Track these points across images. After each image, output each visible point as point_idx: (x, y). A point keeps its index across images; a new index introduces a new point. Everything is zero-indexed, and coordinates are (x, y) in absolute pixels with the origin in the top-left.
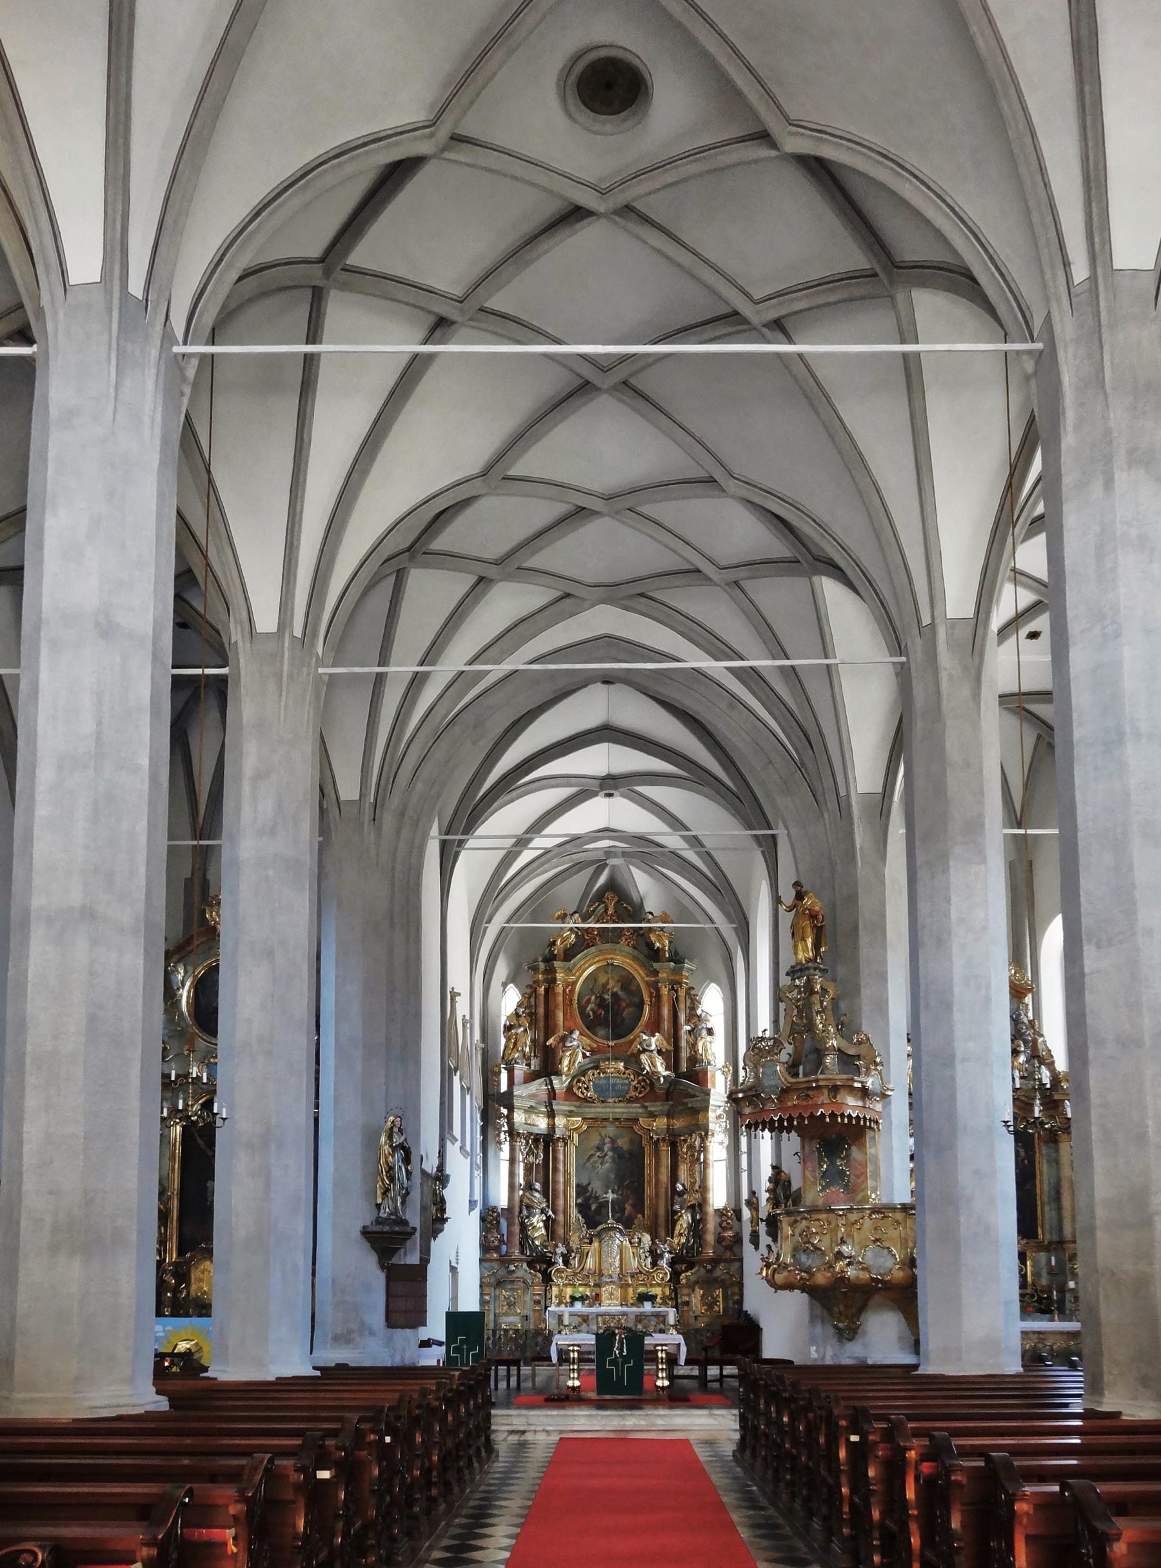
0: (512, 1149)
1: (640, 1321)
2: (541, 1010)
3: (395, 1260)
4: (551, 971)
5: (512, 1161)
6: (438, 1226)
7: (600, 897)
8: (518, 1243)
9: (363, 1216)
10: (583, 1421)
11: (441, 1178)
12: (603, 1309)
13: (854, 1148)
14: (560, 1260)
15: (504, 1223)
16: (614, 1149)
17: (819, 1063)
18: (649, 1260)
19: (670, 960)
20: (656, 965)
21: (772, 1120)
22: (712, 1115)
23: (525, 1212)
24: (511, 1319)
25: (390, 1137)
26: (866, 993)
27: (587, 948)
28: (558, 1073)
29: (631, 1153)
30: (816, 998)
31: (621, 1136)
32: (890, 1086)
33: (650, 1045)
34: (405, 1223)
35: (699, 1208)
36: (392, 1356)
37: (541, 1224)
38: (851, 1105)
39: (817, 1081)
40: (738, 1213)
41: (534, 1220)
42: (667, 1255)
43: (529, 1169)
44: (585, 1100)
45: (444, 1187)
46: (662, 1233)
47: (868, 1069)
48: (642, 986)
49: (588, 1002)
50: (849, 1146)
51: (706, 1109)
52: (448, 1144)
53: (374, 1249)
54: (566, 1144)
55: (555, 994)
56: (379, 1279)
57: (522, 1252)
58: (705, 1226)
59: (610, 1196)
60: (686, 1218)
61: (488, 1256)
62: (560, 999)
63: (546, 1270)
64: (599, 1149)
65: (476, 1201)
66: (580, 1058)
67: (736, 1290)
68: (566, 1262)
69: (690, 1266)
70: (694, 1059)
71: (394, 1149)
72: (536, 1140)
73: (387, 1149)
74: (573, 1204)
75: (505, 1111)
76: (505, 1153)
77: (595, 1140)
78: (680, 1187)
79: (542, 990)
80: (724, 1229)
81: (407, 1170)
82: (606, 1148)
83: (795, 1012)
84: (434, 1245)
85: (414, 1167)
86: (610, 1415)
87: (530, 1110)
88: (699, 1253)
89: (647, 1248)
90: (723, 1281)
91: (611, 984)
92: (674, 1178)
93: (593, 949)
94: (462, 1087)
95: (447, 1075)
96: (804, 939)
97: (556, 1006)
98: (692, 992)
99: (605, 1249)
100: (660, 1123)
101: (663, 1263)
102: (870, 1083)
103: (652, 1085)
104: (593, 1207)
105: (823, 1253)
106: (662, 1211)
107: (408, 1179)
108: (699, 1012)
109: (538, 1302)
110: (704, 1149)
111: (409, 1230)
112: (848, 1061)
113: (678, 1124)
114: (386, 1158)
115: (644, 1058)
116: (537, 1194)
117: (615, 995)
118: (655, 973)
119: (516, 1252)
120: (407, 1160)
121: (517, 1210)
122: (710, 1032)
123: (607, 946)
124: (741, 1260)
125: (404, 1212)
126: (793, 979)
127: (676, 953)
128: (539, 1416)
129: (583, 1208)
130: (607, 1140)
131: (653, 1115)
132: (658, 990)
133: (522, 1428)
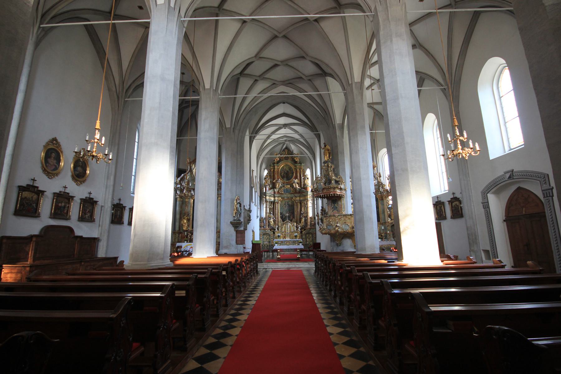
0: (266, 205)
1: (294, 242)
2: (272, 175)
3: (237, 229)
4: (274, 166)
5: (266, 207)
6: (249, 221)
7: (284, 150)
8: (267, 225)
9: (231, 219)
10: (280, 266)
11: (250, 211)
12: (286, 240)
13: (339, 202)
14: (276, 229)
15: (265, 221)
16: (288, 204)
17: (330, 182)
18: (296, 229)
19: (299, 163)
20: (296, 165)
21: (321, 196)
22: (308, 196)
23: (269, 218)
24: (266, 242)
25: (237, 201)
26: (340, 167)
27: (282, 161)
28: (276, 188)
29: (292, 205)
30: (329, 168)
31: (289, 202)
32: (347, 188)
33: (295, 182)
34: (240, 220)
35: (307, 216)
36: (237, 251)
37: (273, 221)
38: (338, 192)
39: (330, 186)
40: (315, 218)
41: (271, 220)
42: (300, 227)
43: (270, 209)
44: (282, 194)
45: (250, 213)
46: (298, 222)
47: (341, 183)
48: (293, 169)
49: (282, 173)
51: (307, 195)
52: (252, 203)
53: (233, 226)
54: (278, 203)
55: (275, 171)
56: (235, 233)
57: (269, 227)
58: (308, 220)
59: (287, 215)
60: (303, 220)
61: (261, 228)
62: (276, 172)
63: (274, 231)
64: (285, 204)
65: (258, 216)
66: (280, 185)
67: (315, 235)
68: (278, 229)
69: (305, 230)
70: (305, 184)
71: (237, 204)
72: (271, 202)
73: (236, 204)
74: (279, 217)
75: (265, 196)
76: (265, 206)
77: (284, 202)
78: (302, 212)
79: (272, 170)
80: (312, 222)
81: (240, 208)
82: (286, 204)
83: (325, 171)
84: (248, 226)
85: (242, 208)
86: (286, 264)
87: (270, 196)
88: (307, 227)
89: (295, 226)
90: (312, 233)
91: (287, 169)
92: (301, 210)
93: (283, 161)
94: (255, 191)
95: (251, 188)
96: (327, 155)
97: (275, 174)
98: (304, 170)
99: (286, 226)
100: (298, 198)
101: (299, 229)
102: (342, 187)
103: (296, 190)
104: (284, 217)
105: (333, 226)
106: (298, 218)
107: (241, 210)
108: (305, 174)
109: (272, 238)
110: (307, 204)
111: (241, 222)
112: (337, 182)
113: (301, 199)
114: (236, 206)
115: (294, 184)
116: (272, 215)
117: (287, 171)
118: (296, 166)
119: (267, 228)
120: (240, 206)
121: (267, 218)
122: (308, 179)
123: (285, 161)
124: (316, 228)
125: (240, 218)
126: (324, 164)
127: (300, 162)
128: (270, 265)
129: (282, 217)
130: (286, 202)
131: (296, 197)
132: (297, 170)
133: (266, 268)
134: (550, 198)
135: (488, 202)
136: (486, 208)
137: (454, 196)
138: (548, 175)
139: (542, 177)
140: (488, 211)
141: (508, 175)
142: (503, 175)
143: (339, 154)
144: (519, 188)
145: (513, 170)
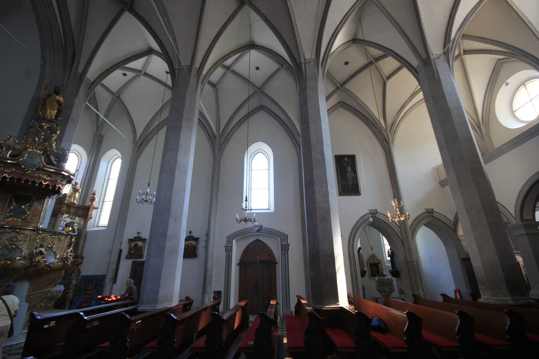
50: (34, 201)
134: (286, 251)
135: (232, 247)
136: (228, 252)
137: (190, 235)
138: (287, 235)
139: (283, 236)
140: (230, 255)
141: (257, 229)
142: (252, 228)
143: (70, 121)
144: (258, 240)
145: (262, 226)
